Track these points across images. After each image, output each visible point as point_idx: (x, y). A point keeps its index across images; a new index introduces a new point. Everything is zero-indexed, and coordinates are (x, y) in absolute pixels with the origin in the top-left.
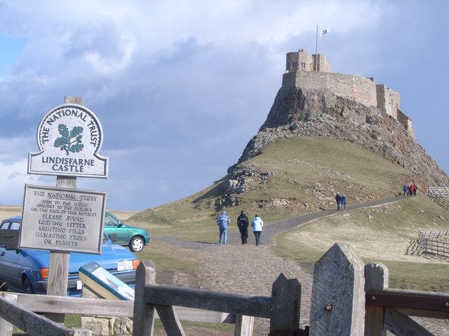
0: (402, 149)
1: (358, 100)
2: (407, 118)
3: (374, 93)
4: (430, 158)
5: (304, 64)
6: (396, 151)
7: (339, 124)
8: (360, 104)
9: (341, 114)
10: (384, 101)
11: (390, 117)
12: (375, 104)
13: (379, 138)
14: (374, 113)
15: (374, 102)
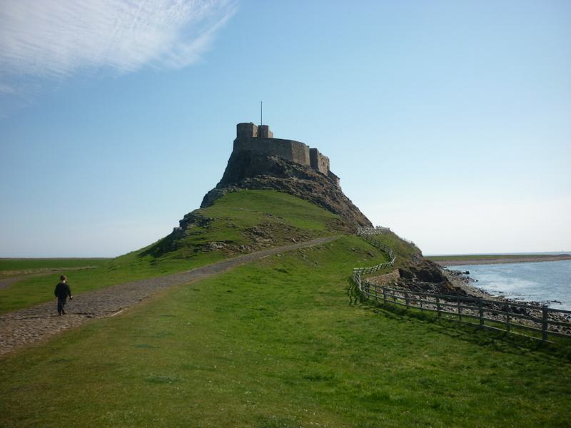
0: (334, 199)
1: (296, 161)
2: (336, 177)
3: (308, 155)
4: (354, 206)
5: (252, 133)
6: (328, 200)
7: (280, 179)
8: (296, 164)
9: (282, 172)
10: (317, 162)
11: (323, 174)
12: (309, 164)
13: (314, 190)
14: (310, 172)
15: (308, 162)
